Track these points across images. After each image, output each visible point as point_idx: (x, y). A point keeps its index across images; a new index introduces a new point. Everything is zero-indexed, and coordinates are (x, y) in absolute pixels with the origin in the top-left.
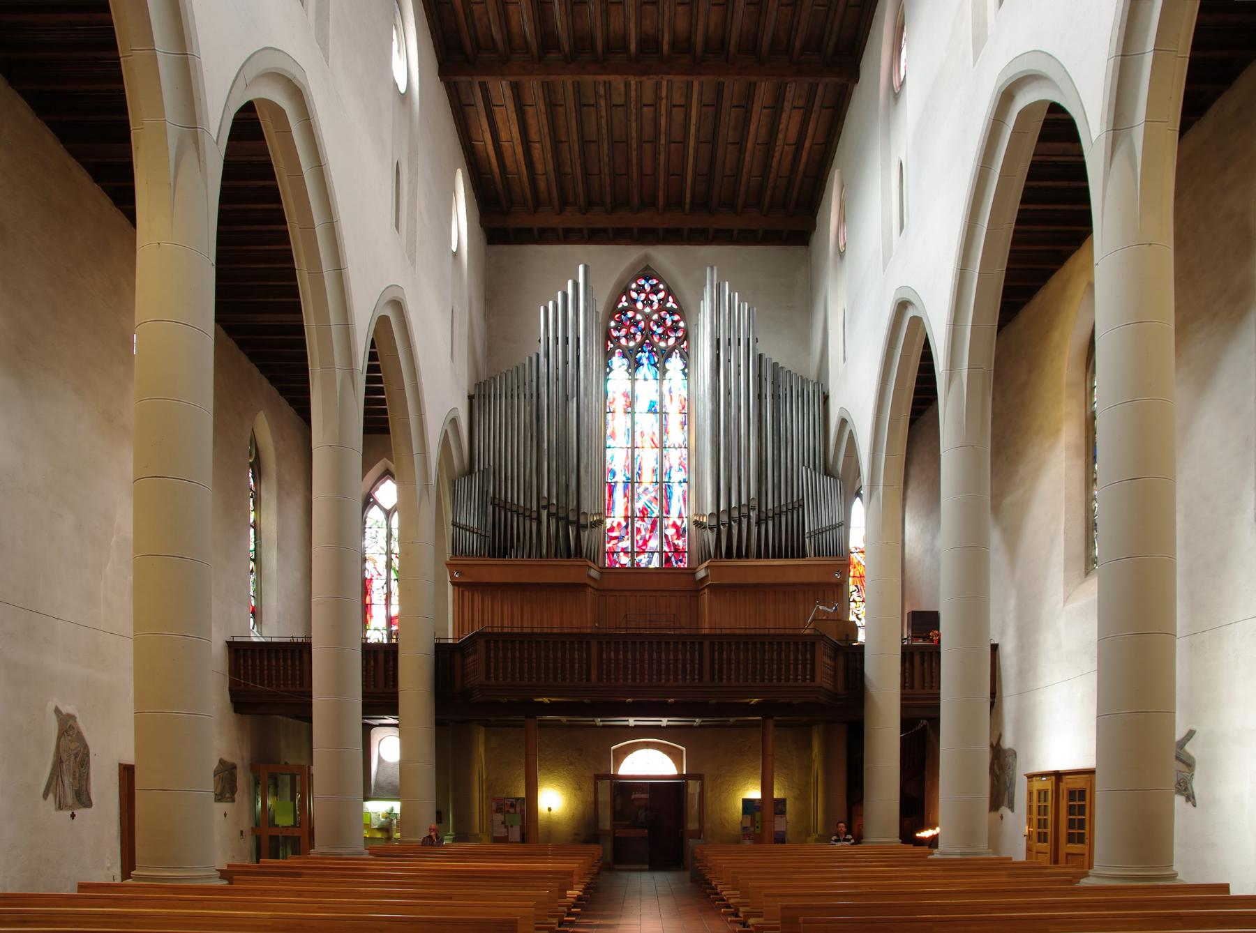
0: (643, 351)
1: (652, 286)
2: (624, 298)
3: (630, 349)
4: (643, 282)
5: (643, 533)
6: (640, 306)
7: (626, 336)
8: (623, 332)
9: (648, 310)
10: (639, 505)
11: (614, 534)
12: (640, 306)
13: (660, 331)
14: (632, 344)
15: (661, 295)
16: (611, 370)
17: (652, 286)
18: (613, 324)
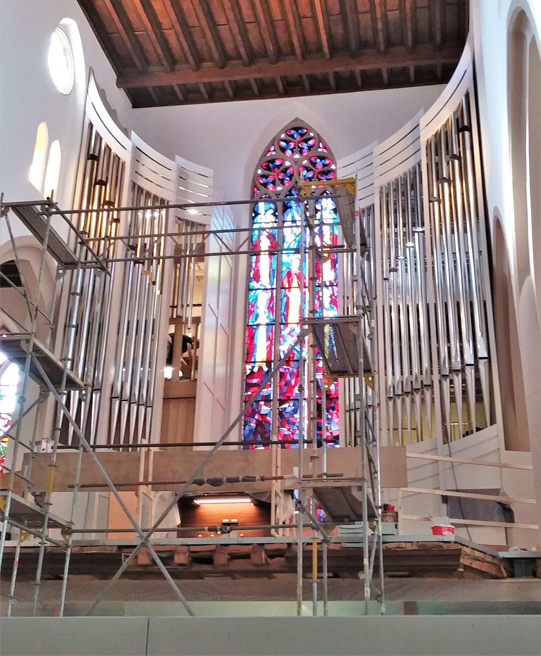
0: (291, 194)
1: (302, 135)
2: (272, 148)
3: (278, 194)
4: (293, 132)
5: (288, 378)
6: (289, 152)
7: (274, 183)
8: (270, 179)
9: (297, 156)
10: (284, 348)
11: (255, 381)
12: (289, 152)
13: (310, 175)
14: (279, 188)
15: (311, 142)
16: (257, 214)
17: (302, 135)
18: (259, 172)
